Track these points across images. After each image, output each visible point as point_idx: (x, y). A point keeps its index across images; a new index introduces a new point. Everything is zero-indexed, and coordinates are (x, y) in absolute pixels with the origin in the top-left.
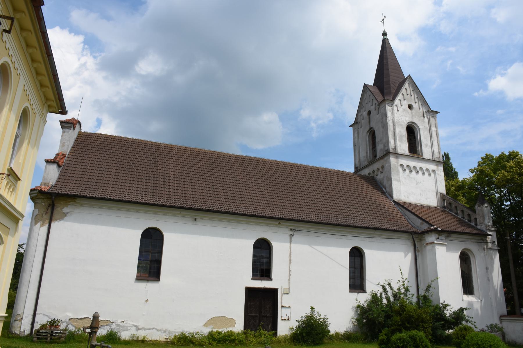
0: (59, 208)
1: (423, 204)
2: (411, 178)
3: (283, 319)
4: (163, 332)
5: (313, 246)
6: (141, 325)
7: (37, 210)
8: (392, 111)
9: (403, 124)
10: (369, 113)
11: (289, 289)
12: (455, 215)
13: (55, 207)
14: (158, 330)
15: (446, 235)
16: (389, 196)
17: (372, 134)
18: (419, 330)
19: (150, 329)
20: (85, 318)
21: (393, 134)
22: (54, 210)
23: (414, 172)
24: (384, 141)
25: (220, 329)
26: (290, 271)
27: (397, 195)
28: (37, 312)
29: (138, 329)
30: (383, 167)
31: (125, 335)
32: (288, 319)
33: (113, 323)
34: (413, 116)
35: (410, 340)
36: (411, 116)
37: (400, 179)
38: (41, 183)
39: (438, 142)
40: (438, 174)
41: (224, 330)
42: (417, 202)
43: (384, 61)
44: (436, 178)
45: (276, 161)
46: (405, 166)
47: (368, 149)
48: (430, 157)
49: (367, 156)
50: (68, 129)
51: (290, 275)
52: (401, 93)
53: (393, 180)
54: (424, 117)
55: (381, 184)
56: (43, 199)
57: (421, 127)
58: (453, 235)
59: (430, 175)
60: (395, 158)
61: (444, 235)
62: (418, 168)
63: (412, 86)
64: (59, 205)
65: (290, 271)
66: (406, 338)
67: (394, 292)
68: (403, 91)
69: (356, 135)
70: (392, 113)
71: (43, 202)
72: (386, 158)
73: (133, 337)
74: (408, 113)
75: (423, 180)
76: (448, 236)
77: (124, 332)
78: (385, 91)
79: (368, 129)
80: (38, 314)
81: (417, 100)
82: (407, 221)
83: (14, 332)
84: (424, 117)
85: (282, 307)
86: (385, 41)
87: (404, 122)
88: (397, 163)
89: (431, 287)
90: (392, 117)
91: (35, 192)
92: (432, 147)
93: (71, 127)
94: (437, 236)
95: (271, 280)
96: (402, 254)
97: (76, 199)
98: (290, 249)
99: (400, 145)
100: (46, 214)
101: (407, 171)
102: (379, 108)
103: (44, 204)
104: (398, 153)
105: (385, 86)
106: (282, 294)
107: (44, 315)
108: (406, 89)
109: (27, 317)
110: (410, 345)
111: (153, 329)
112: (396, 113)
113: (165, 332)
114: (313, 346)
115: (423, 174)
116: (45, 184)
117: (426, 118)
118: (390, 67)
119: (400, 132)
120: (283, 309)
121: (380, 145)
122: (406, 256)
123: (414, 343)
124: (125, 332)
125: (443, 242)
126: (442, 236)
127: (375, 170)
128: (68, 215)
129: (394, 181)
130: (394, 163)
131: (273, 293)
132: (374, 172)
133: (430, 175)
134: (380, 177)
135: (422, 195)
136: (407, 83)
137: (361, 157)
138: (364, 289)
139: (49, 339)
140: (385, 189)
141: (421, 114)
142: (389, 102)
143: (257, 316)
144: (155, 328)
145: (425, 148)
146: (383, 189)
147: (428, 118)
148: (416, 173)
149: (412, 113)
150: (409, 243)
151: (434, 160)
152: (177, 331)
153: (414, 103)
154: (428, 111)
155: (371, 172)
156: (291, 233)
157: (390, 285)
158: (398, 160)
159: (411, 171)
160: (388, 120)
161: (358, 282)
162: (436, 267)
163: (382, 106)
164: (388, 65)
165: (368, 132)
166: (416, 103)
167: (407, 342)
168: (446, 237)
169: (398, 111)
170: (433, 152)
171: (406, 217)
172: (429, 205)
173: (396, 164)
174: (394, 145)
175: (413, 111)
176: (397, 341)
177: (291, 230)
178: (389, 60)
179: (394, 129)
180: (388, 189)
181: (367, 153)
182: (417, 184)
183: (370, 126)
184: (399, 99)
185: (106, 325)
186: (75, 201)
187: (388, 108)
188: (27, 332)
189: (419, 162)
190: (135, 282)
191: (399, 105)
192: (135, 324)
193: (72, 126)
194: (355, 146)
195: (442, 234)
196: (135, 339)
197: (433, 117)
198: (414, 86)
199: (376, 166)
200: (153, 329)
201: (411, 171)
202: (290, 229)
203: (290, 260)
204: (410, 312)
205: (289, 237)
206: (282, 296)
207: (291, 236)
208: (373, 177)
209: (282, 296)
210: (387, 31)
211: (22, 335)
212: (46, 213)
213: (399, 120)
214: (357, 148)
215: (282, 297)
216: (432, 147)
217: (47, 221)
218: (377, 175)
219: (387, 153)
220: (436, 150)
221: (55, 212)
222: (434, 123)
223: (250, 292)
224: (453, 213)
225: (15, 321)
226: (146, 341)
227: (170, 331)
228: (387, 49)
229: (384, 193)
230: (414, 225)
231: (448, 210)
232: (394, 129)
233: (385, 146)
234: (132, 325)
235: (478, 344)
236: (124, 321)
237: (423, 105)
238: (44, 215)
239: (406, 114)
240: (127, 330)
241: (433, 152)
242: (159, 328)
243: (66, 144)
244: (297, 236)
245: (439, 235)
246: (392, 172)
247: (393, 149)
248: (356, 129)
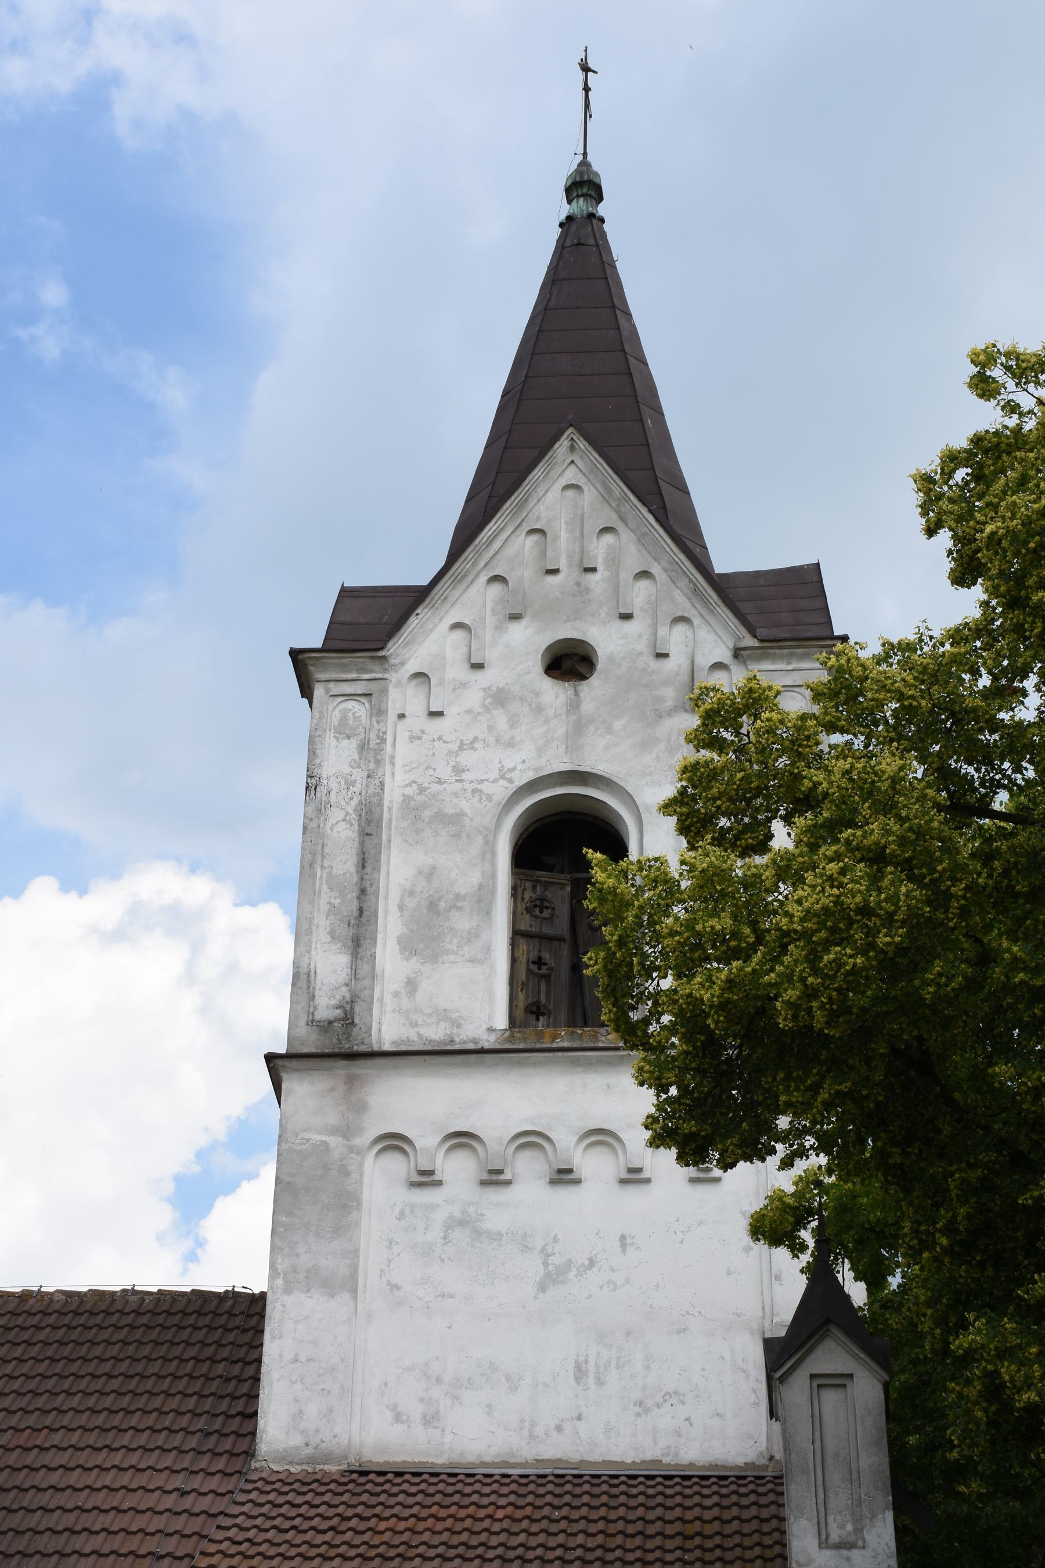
1: (596, 1456)
2: (496, 1237)
9: (465, 806)
27: (298, 1415)
34: (578, 728)
36: (561, 731)
37: (353, 1276)
62: (565, 1139)
70: (363, 747)
74: (539, 709)
75: (623, 1238)
87: (486, 787)
90: (359, 775)
99: (412, 985)
104: (363, 1048)
130: (316, 1137)
135: (591, 1380)
142: (344, 668)
149: (574, 705)
158: (361, 1108)
172: (666, 1460)
173: (334, 1141)
175: (593, 689)
182: (551, 1279)
191: (456, 670)
213: (435, 788)
237: (696, 621)
247: (330, 1022)
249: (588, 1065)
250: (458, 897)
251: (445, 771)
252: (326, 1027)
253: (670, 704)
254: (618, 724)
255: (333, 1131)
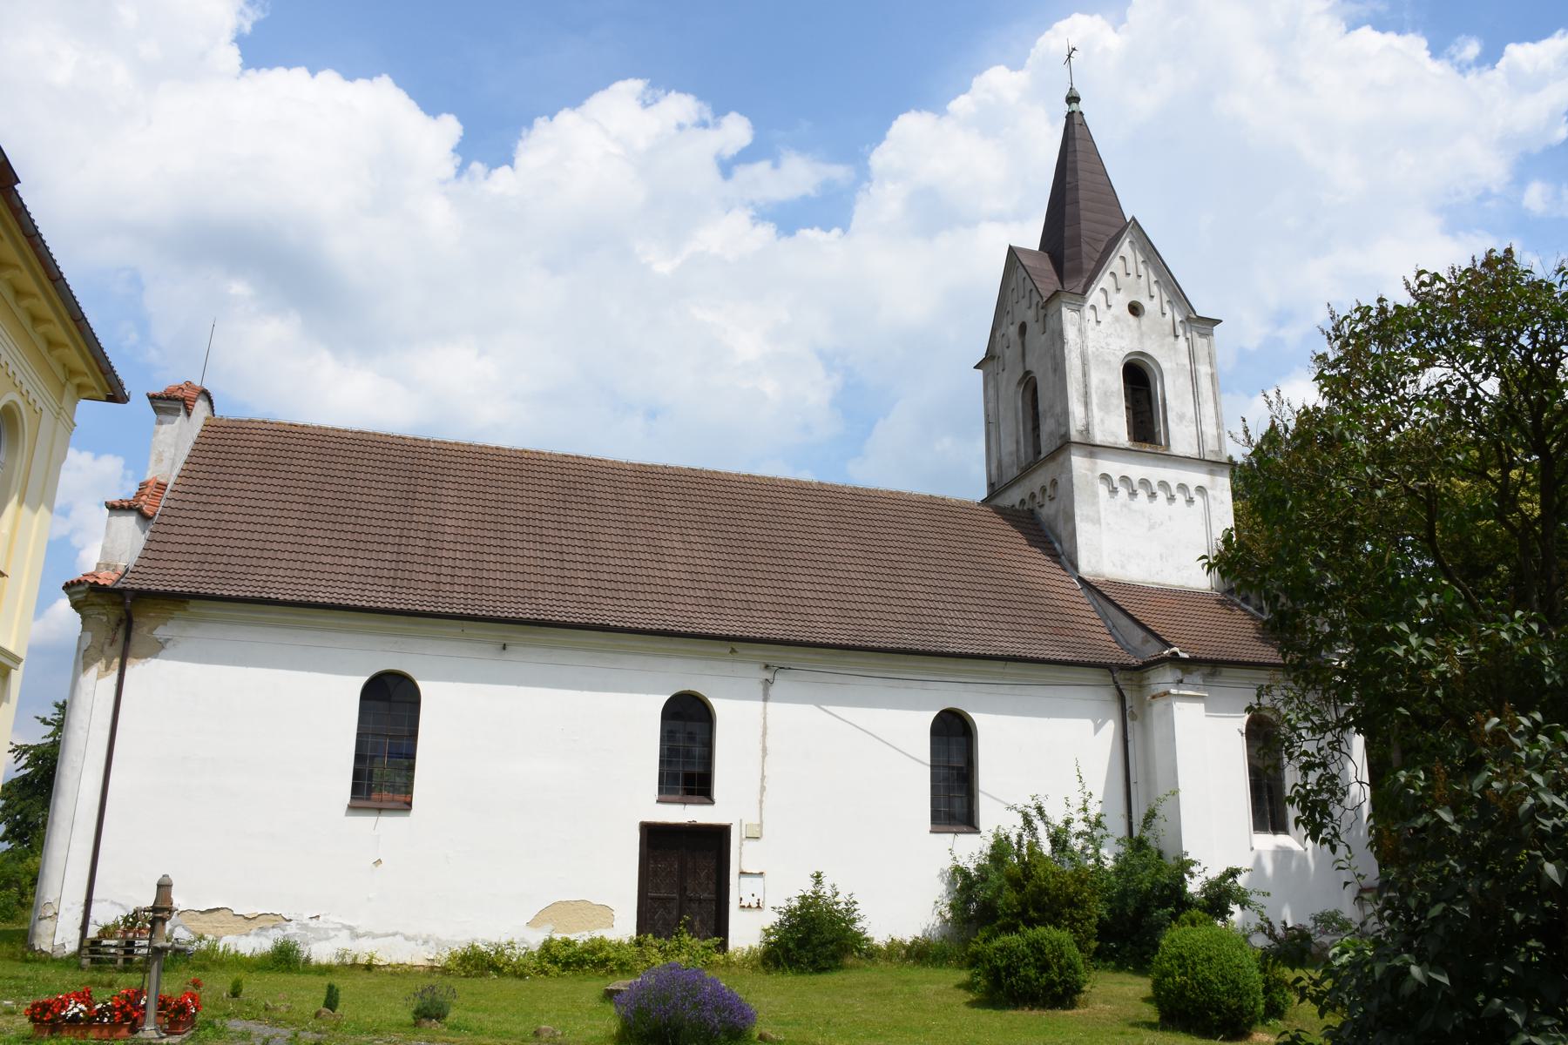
0: (145, 629)
3: (743, 907)
4: (420, 942)
5: (830, 708)
6: (362, 925)
7: (89, 635)
8: (1080, 324)
9: (1112, 358)
10: (1023, 328)
11: (761, 825)
12: (1253, 615)
13: (134, 626)
14: (407, 938)
15: (1207, 670)
16: (1068, 565)
17: (1029, 385)
18: (1058, 926)
19: (387, 935)
20: (218, 909)
21: (1082, 390)
22: (133, 634)
23: (1142, 494)
24: (1058, 410)
25: (571, 933)
26: (763, 778)
27: (1089, 562)
28: (95, 896)
29: (355, 935)
30: (1054, 483)
31: (321, 952)
32: (758, 907)
33: (290, 920)
34: (1142, 335)
35: (1028, 951)
38: (98, 564)
39: (1216, 407)
40: (1215, 499)
41: (581, 937)
42: (1151, 580)
43: (1068, 179)
44: (1207, 508)
45: (749, 476)
46: (1116, 478)
47: (1021, 433)
48: (1192, 451)
49: (1018, 450)
50: (171, 414)
51: (763, 789)
52: (1108, 272)
53: (1077, 519)
54: (1176, 336)
55: (1053, 531)
56: (103, 605)
57: (1165, 365)
58: (1226, 671)
59: (1190, 501)
60: (1085, 456)
61: (1199, 673)
62: (1155, 484)
63: (1143, 251)
64: (143, 620)
65: (763, 778)
66: (1019, 946)
67: (1051, 830)
68: (1115, 264)
69: (991, 392)
71: (103, 614)
72: (1061, 459)
73: (343, 956)
74: (1129, 326)
76: (1213, 674)
77: (320, 943)
78: (1067, 265)
79: (1020, 374)
80: (97, 901)
81: (1155, 289)
82: (1111, 634)
83: (37, 948)
84: (1176, 336)
85: (742, 873)
86: (1073, 118)
88: (1093, 470)
89: (1155, 815)
90: (1078, 341)
91: (81, 588)
92: (1198, 422)
93: (179, 410)
94: (1179, 675)
95: (712, 802)
96: (1088, 724)
97: (188, 603)
98: (765, 718)
99: (1102, 421)
100: (111, 645)
101: (1123, 492)
102: (1045, 315)
103: (105, 618)
105: (1067, 252)
106: (741, 840)
107: (113, 903)
108: (1123, 258)
109: (70, 909)
110: (1027, 965)
111: (394, 934)
112: (1092, 329)
113: (426, 942)
114: (811, 974)
115: (1168, 499)
116: (108, 566)
117: (1182, 339)
118: (1082, 194)
119: (1103, 381)
120: (744, 880)
121: (1048, 421)
122: (1097, 729)
123: (1037, 960)
124: (323, 944)
125: (1198, 690)
126: (1195, 674)
127: (1037, 491)
128: (168, 645)
129: (1082, 520)
130: (1084, 471)
131: (717, 838)
132: (1033, 496)
133: (1190, 501)
134: (1047, 511)
136: (1128, 240)
137: (1003, 454)
138: (976, 825)
139: (120, 961)
140: (1061, 544)
141: (1169, 329)
143: (674, 899)
144: (400, 931)
145: (1178, 425)
146: (1057, 545)
147: (1187, 339)
148: (1149, 496)
149: (1139, 327)
150: (1108, 694)
151: (1204, 460)
152: (458, 939)
153: (1148, 298)
154: (1188, 319)
155: (1027, 498)
156: (768, 675)
157: (1040, 810)
158: (1096, 463)
159: (1133, 494)
160: (1066, 351)
161: (958, 806)
162: (1175, 760)
163: (1052, 309)
164: (1077, 190)
165: (1019, 383)
166: (1152, 297)
167: (1018, 957)
168: (1205, 677)
169: (1098, 322)
170: (1200, 436)
171: (1109, 623)
173: (1089, 473)
174: (1084, 421)
175: (1144, 319)
176: (995, 954)
177: (767, 667)
178: (1081, 174)
179: (1085, 374)
180: (1066, 546)
181: (1018, 442)
182: (1151, 527)
183: (1024, 368)
184: (1102, 289)
185: (273, 927)
186: (185, 610)
187: (1068, 315)
188: (72, 947)
189: (1157, 466)
190: (346, 815)
191: (1102, 306)
192: (347, 923)
193: (182, 407)
194: (988, 423)
195: (1194, 668)
196: (349, 960)
197: (1201, 335)
198: (1149, 247)
199: (1040, 479)
200: (394, 934)
201: (1133, 494)
202: (763, 666)
203: (764, 750)
204: (1040, 878)
205: (761, 687)
206: (741, 844)
207: (768, 683)
208: (1032, 511)
209: (741, 844)
210: (1080, 91)
211: (58, 954)
212: (113, 642)
214: (992, 428)
215: (740, 848)
216: (1198, 422)
217: (117, 661)
218: (1042, 506)
219: (1065, 445)
220: (1210, 430)
221: (135, 637)
222: (1206, 353)
223: (655, 837)
224: (1251, 609)
225: (40, 919)
226: (379, 966)
227: (438, 939)
228: (1077, 142)
229: (1055, 556)
230: (1128, 643)
231: (1238, 601)
232: (1085, 374)
233: (1059, 424)
234: (339, 926)
235: (1181, 956)
236: (318, 916)
238: (106, 647)
239: (1122, 330)
240: (328, 939)
241: (1200, 436)
242: (410, 932)
243: (168, 454)
244: (782, 683)
245: (1186, 671)
246: (1076, 498)
248: (990, 377)
249: (1159, 459)
250: (1112, 392)
251: (1104, 345)
252: (1081, 432)
253: (1167, 332)
254: (1153, 337)
255: (1088, 470)
